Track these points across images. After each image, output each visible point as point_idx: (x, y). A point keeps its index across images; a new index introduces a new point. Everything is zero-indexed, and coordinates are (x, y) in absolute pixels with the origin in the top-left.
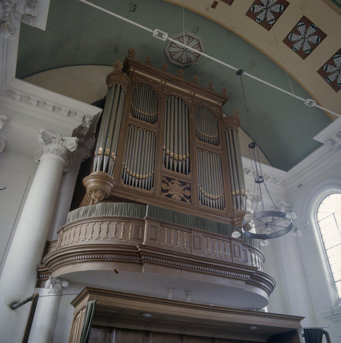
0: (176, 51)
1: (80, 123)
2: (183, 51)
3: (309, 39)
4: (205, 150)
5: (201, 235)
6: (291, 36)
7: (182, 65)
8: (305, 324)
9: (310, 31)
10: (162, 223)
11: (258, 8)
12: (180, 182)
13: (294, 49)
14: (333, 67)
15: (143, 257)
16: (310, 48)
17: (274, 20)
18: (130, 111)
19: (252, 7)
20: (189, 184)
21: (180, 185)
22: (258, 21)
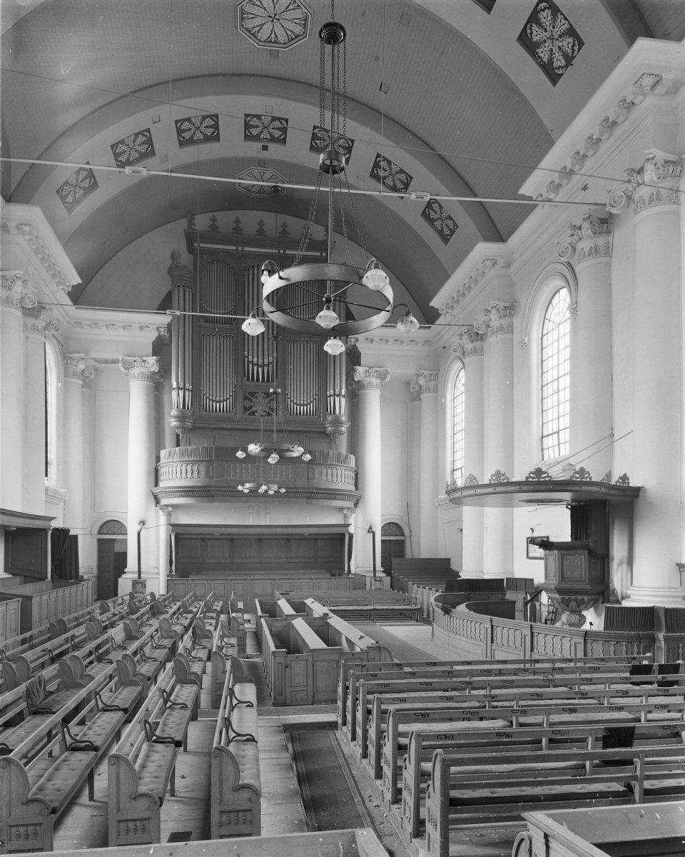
1: (157, 334)
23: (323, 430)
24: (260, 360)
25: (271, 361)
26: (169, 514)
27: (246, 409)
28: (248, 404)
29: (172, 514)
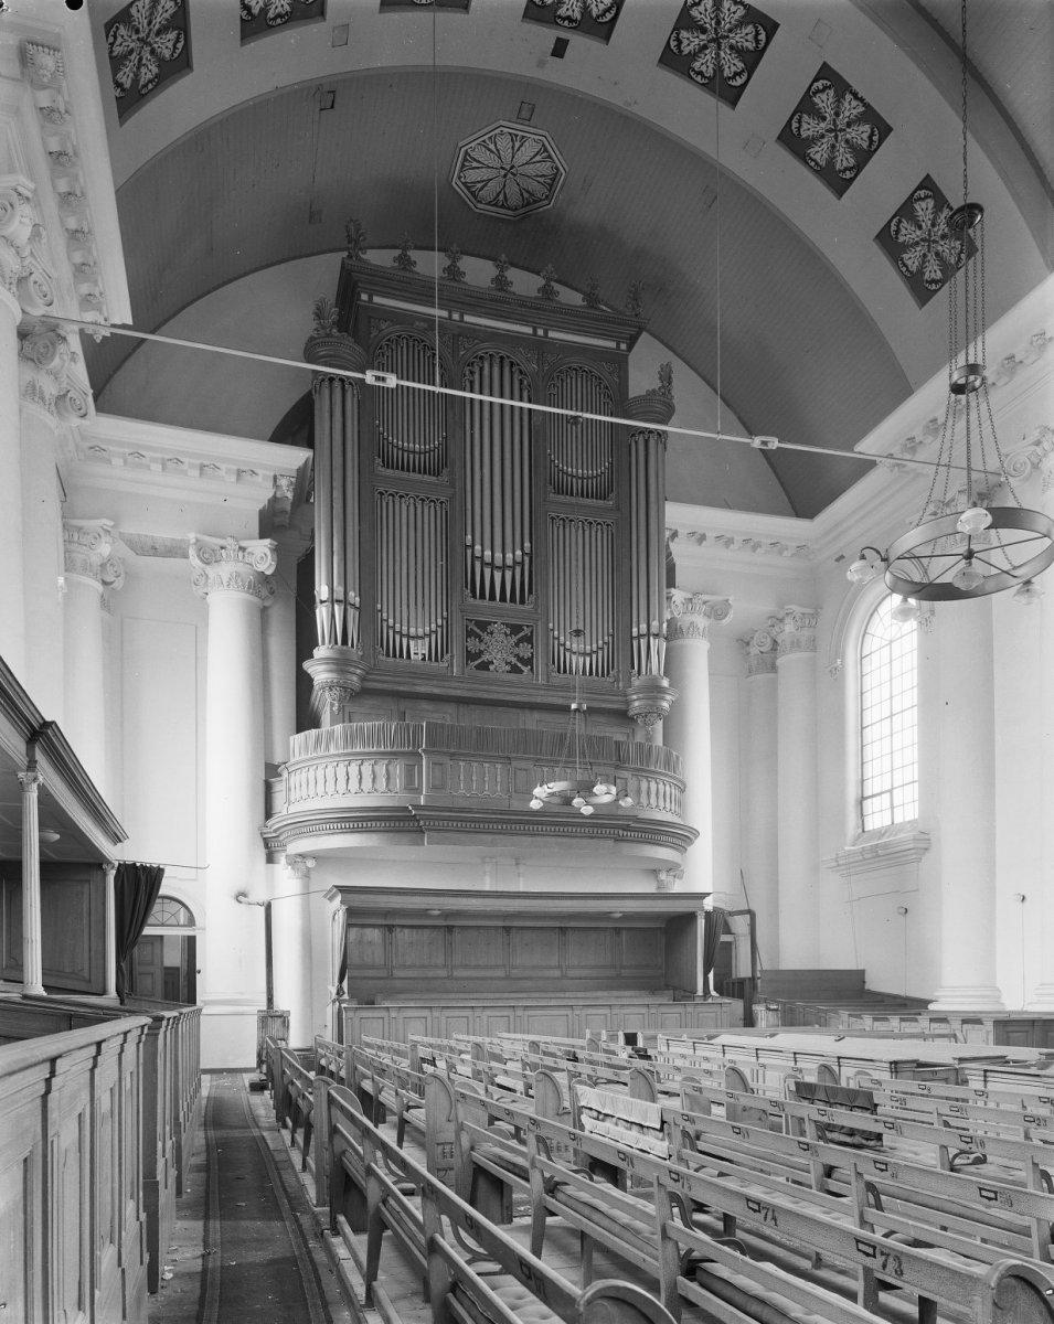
0: (486, 163)
1: (271, 495)
2: (505, 176)
3: (849, 133)
4: (571, 521)
5: (530, 765)
6: (800, 122)
7: (510, 213)
8: (708, 904)
9: (849, 110)
10: (453, 754)
11: (690, 41)
12: (507, 625)
13: (813, 164)
14: (913, 229)
15: (422, 823)
16: (852, 162)
17: (746, 74)
18: (376, 452)
19: (673, 38)
20: (528, 626)
21: (508, 632)
22: (699, 79)
23: (623, 707)
24: (498, 555)
25: (519, 559)
26: (307, 875)
27: (471, 656)
28: (473, 645)
29: (313, 875)
